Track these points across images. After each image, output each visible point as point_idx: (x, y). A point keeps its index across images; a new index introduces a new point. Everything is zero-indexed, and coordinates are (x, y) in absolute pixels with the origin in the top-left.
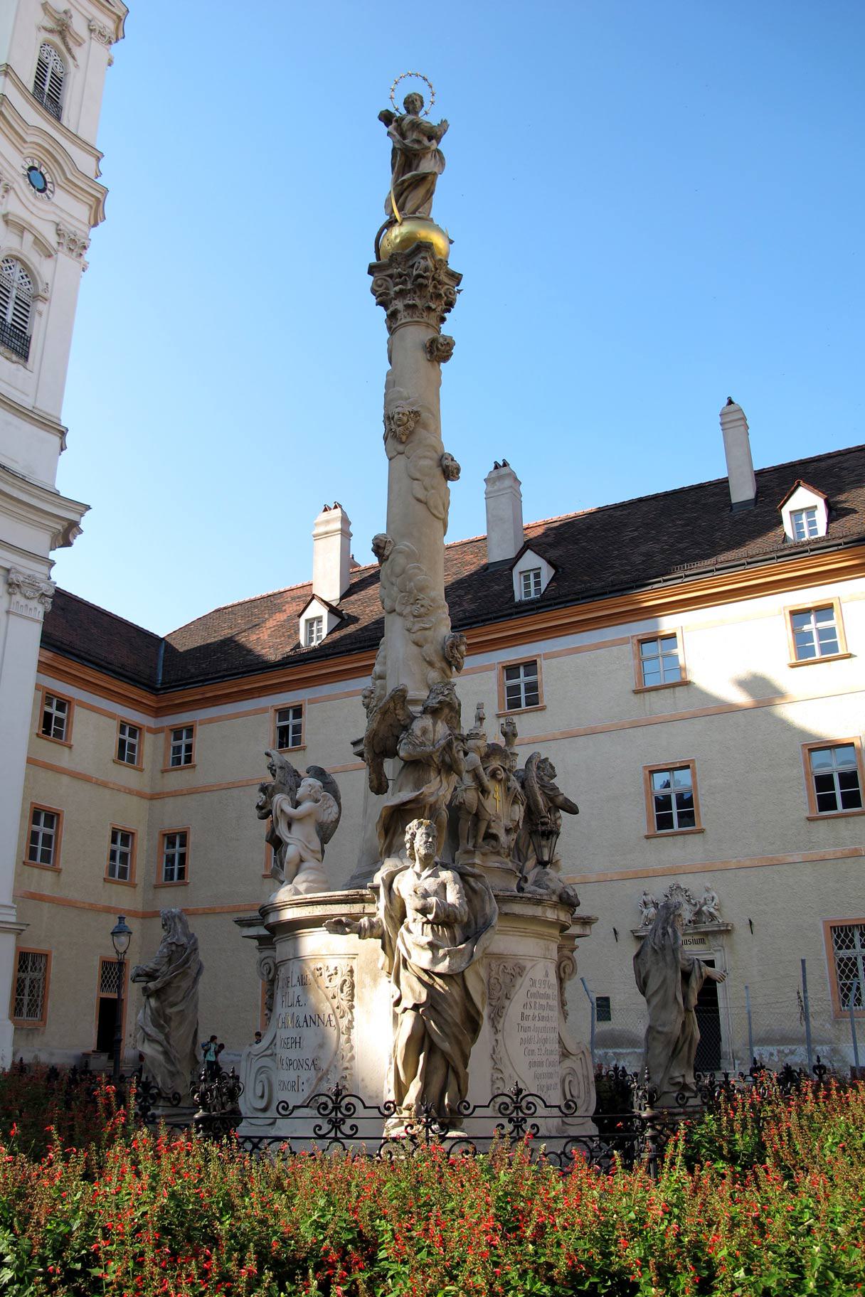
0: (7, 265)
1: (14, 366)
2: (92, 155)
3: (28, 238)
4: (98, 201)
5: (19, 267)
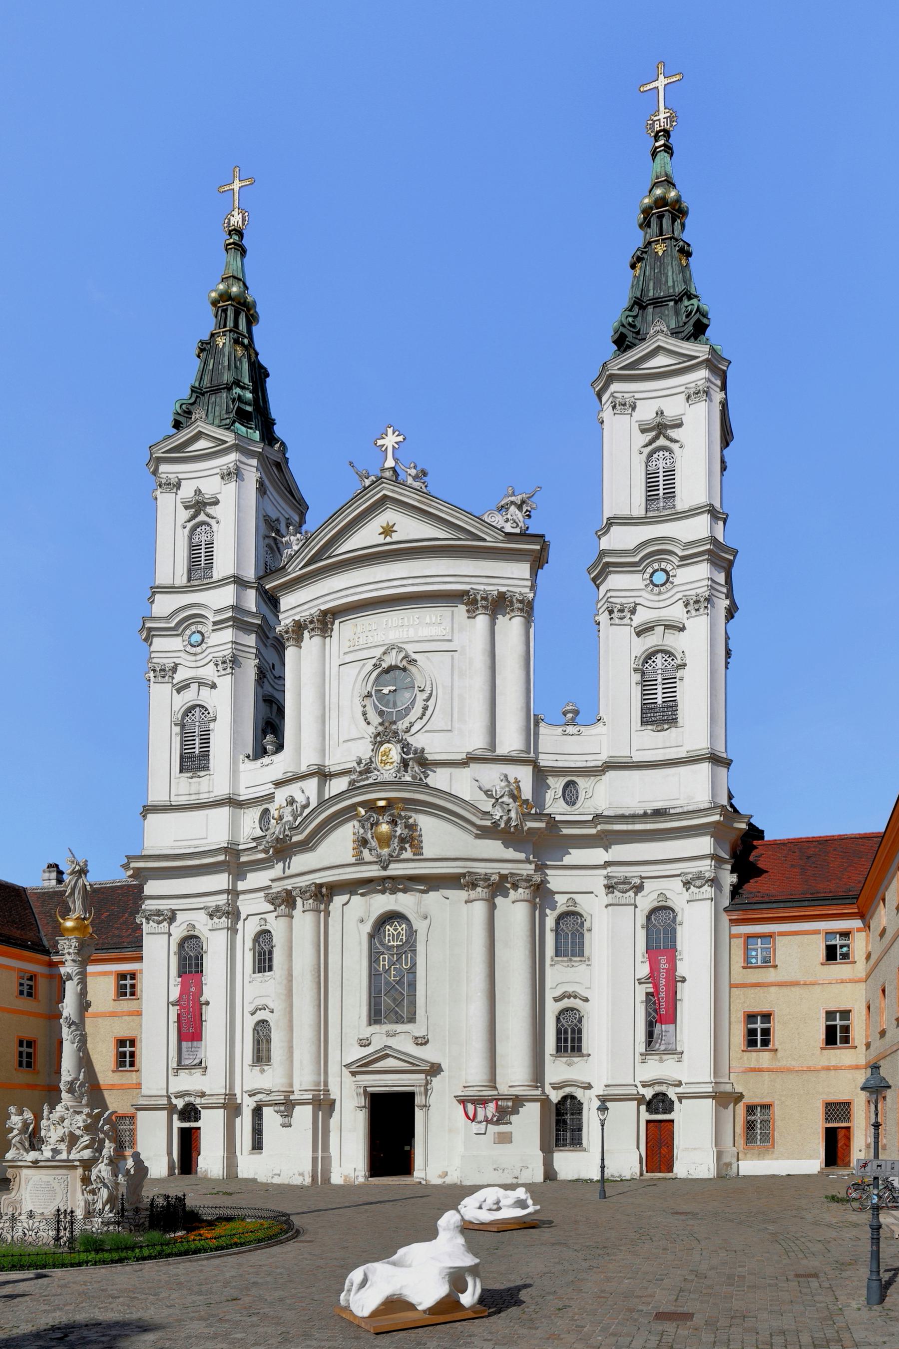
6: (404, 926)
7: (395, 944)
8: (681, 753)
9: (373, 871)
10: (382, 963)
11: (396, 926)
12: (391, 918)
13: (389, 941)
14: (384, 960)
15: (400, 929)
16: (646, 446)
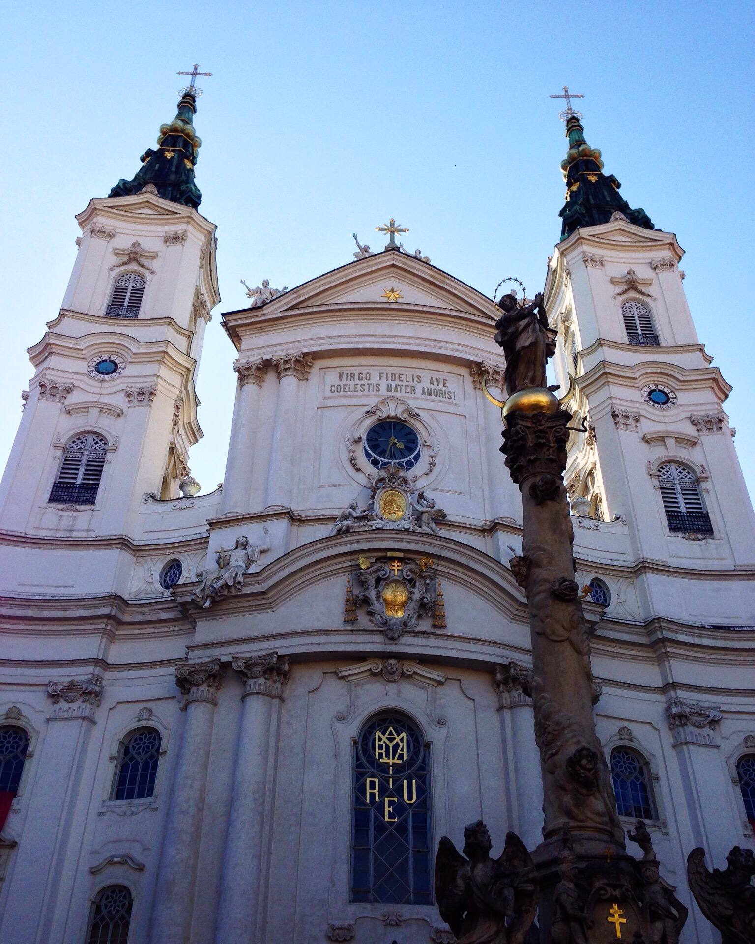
0: (663, 471)
1: (703, 542)
2: (693, 351)
3: (670, 442)
4: (715, 380)
5: (673, 466)
6: (404, 735)
7: (391, 761)
8: (727, 564)
9: (374, 644)
10: (368, 791)
11: (391, 733)
12: (384, 721)
13: (381, 755)
14: (372, 785)
15: (398, 739)
16: (619, 294)
